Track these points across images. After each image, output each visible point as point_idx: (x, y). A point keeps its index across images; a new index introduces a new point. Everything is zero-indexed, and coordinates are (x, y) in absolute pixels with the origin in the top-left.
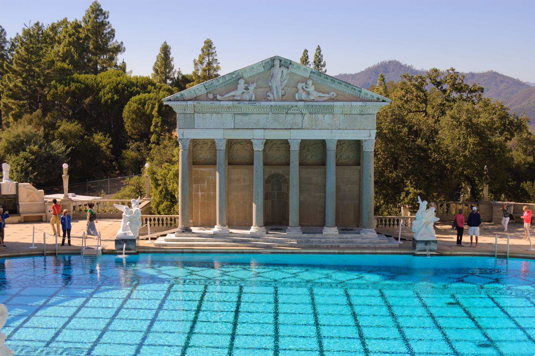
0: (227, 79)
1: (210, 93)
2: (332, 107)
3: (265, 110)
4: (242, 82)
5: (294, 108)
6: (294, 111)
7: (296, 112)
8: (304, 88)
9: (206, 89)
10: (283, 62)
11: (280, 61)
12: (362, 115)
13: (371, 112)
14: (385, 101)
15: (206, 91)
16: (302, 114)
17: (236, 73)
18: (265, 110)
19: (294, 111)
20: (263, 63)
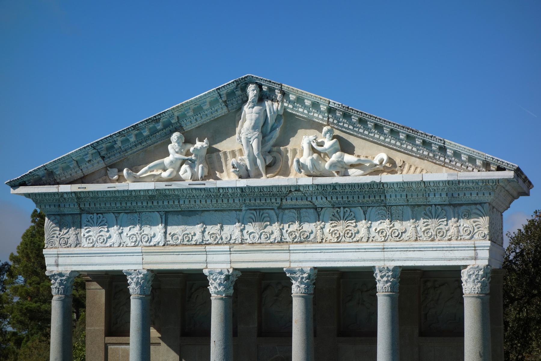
0: (146, 133)
1: (112, 166)
2: (379, 189)
3: (231, 201)
4: (175, 136)
5: (295, 194)
6: (294, 202)
7: (300, 203)
8: (314, 145)
9: (103, 158)
10: (265, 88)
11: (260, 86)
12: (455, 205)
13: (474, 197)
14: (504, 169)
15: (102, 164)
16: (316, 208)
17: (163, 120)
18: (231, 201)
19: (294, 202)
20: (224, 92)
